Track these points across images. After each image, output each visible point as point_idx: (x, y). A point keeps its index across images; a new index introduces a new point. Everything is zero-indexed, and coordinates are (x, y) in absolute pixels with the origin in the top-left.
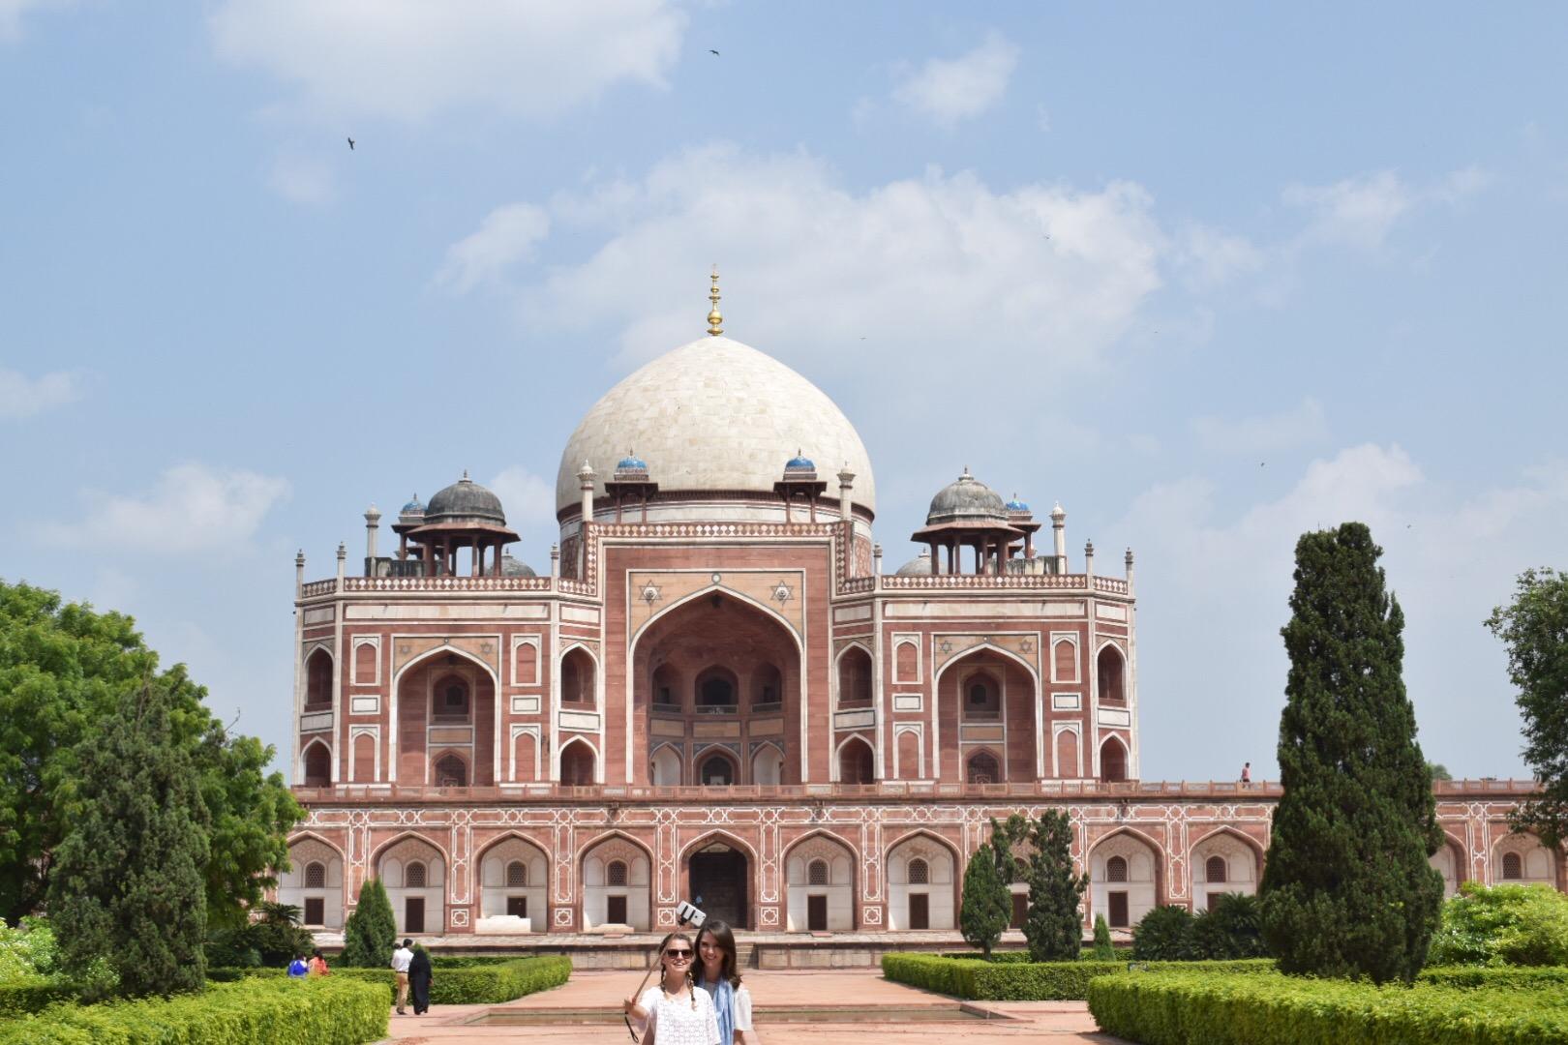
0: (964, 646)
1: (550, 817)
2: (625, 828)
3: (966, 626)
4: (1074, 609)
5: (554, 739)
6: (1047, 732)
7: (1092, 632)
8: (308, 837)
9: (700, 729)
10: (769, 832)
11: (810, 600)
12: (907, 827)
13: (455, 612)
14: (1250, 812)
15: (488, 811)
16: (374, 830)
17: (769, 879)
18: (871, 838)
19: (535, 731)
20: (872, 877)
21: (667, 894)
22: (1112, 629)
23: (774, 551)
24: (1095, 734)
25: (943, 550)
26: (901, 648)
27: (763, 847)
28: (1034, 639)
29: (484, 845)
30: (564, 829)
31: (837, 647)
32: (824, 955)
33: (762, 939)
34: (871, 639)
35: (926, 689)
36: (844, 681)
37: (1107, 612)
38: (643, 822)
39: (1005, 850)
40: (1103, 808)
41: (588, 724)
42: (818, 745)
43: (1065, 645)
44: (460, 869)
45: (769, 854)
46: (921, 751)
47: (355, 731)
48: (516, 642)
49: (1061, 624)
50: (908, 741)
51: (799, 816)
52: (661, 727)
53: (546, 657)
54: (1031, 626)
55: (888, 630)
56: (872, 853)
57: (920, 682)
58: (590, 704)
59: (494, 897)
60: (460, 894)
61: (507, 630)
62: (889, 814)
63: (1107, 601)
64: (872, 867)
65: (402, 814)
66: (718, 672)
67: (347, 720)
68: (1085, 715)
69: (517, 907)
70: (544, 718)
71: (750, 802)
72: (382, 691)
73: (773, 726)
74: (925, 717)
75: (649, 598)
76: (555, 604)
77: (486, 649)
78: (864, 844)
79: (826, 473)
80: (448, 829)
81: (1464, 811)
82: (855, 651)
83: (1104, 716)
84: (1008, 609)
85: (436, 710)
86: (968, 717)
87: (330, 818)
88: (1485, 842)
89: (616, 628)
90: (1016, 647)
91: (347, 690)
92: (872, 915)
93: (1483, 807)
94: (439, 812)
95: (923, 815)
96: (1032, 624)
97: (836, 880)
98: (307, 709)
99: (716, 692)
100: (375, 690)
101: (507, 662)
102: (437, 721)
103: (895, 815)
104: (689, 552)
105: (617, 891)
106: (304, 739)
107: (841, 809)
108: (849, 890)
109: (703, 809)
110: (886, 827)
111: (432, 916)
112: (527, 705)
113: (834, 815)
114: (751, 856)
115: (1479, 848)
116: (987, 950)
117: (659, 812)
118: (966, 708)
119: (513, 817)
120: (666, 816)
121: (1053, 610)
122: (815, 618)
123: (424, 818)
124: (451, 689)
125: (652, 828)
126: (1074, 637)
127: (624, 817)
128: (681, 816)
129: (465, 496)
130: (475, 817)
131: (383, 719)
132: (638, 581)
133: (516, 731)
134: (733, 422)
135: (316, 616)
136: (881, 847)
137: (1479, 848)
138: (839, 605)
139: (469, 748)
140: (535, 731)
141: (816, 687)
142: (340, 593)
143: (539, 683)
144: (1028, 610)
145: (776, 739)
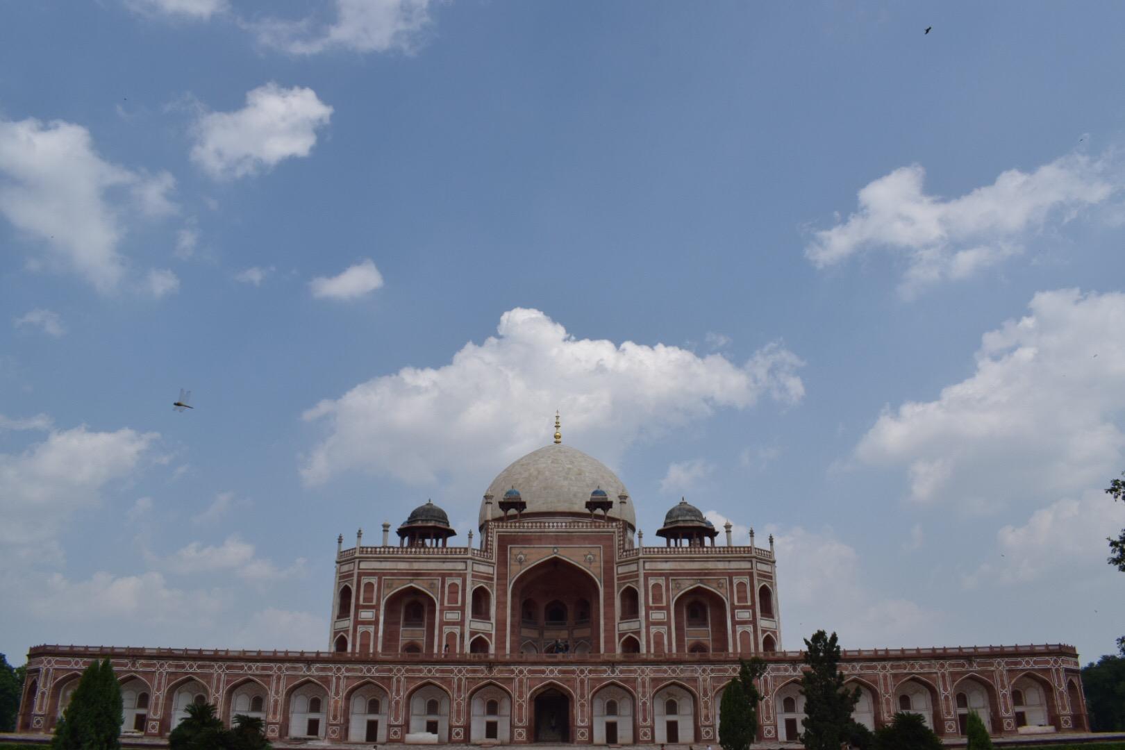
0: (688, 585)
1: (452, 672)
2: (496, 679)
4: (746, 565)
5: (467, 635)
6: (734, 632)
7: (756, 577)
8: (308, 682)
9: (547, 634)
10: (582, 682)
11: (605, 562)
12: (665, 679)
13: (416, 566)
14: (869, 668)
15: (415, 667)
16: (348, 678)
17: (582, 711)
18: (644, 686)
19: (457, 630)
20: (644, 710)
21: (520, 720)
22: (765, 576)
23: (585, 538)
24: (759, 633)
25: (672, 541)
27: (579, 691)
28: (725, 581)
29: (412, 688)
30: (460, 680)
31: (619, 587)
34: (637, 582)
35: (667, 608)
36: (623, 606)
38: (507, 675)
39: (750, 682)
40: (782, 666)
41: (486, 627)
42: (610, 641)
43: (741, 584)
44: (397, 703)
45: (582, 696)
46: (666, 642)
47: (360, 629)
48: (449, 581)
49: (740, 573)
50: (659, 637)
51: (601, 672)
52: (526, 632)
54: (723, 574)
55: (646, 576)
56: (644, 695)
58: (486, 617)
59: (418, 722)
60: (396, 719)
61: (444, 576)
62: (655, 671)
63: (762, 561)
64: (644, 704)
65: (364, 668)
66: (557, 599)
67: (357, 623)
68: (754, 622)
69: (432, 727)
70: (461, 623)
71: (571, 663)
72: (376, 607)
73: (586, 632)
74: (668, 624)
75: (520, 562)
76: (470, 562)
77: (432, 586)
78: (640, 689)
79: (612, 497)
81: (992, 665)
83: (763, 623)
84: (710, 565)
85: (406, 619)
86: (690, 625)
87: (323, 670)
89: (502, 577)
90: (715, 585)
91: (358, 607)
92: (645, 734)
93: (1003, 661)
94: (386, 667)
95: (674, 671)
98: (338, 617)
99: (556, 615)
101: (443, 593)
102: (406, 625)
103: (658, 671)
104: (541, 538)
105: (492, 718)
106: (336, 633)
107: (625, 668)
108: (630, 719)
109: (543, 668)
110: (653, 680)
112: (453, 616)
113: (621, 672)
114: (571, 696)
115: (1003, 687)
117: (516, 668)
118: (688, 620)
119: (430, 671)
120: (521, 672)
121: (734, 565)
122: (608, 572)
123: (377, 671)
124: (412, 606)
125: (512, 679)
126: (746, 580)
127: (496, 673)
129: (428, 510)
131: (376, 623)
132: (515, 551)
133: (447, 630)
134: (565, 479)
135: (345, 568)
136: (650, 691)
137: (1003, 687)
138: (620, 564)
139: (422, 640)
140: (457, 630)
141: (608, 608)
142: (357, 555)
143: (460, 604)
144: (721, 565)
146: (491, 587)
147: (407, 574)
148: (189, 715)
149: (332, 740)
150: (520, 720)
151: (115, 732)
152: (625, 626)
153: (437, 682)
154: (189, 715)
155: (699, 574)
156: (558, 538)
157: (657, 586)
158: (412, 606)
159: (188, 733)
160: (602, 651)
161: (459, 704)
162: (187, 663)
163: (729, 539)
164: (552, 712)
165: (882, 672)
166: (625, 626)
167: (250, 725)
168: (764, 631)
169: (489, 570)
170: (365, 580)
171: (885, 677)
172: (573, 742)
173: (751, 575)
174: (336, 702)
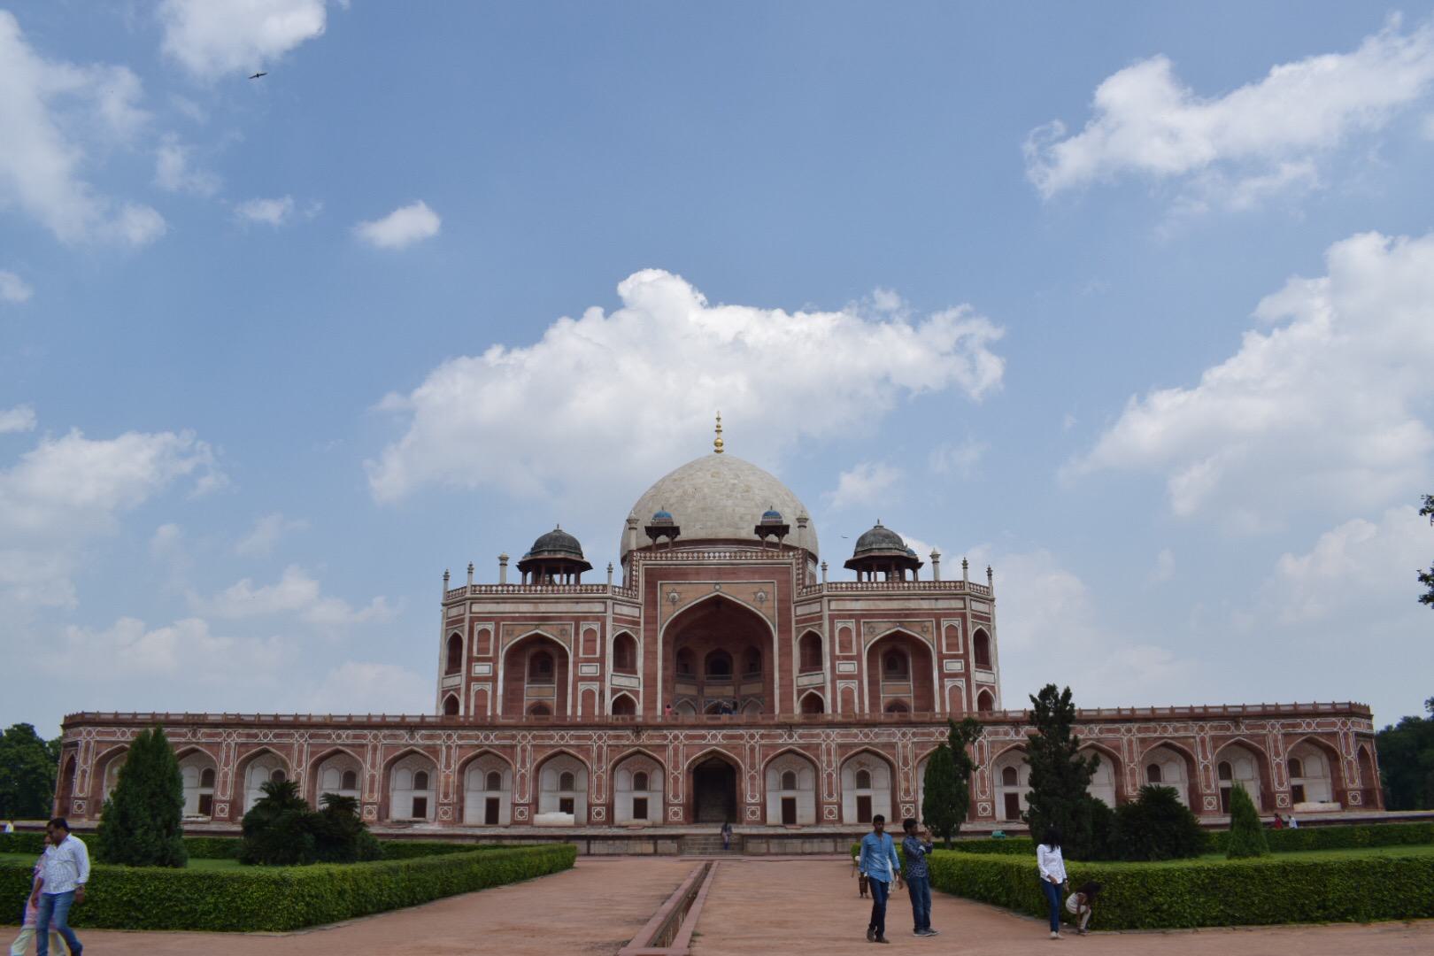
0: (884, 629)
1: (590, 738)
3: (885, 615)
4: (958, 604)
5: (608, 694)
6: (942, 687)
7: (970, 620)
8: (412, 752)
9: (708, 691)
10: (752, 749)
11: (780, 601)
12: (855, 745)
13: (543, 608)
14: (1109, 731)
15: (544, 733)
16: (460, 747)
18: (829, 754)
19: (595, 687)
20: (830, 784)
22: (981, 618)
23: (755, 571)
25: (865, 574)
26: (842, 630)
27: (748, 760)
30: (600, 748)
31: (798, 631)
32: (796, 845)
33: (747, 831)
34: (821, 625)
35: (858, 658)
36: (803, 655)
37: (980, 607)
38: (658, 742)
39: (961, 748)
40: (1001, 729)
41: (632, 683)
43: (951, 628)
44: (523, 777)
45: (753, 766)
47: (475, 687)
48: (584, 627)
49: (949, 614)
50: (847, 693)
51: (775, 737)
52: (681, 689)
53: (603, 637)
54: (929, 615)
55: (832, 618)
56: (830, 763)
57: (854, 653)
59: (549, 799)
60: (522, 796)
61: (577, 620)
62: (842, 736)
64: (830, 775)
65: (481, 735)
66: (720, 647)
68: (967, 675)
69: (567, 806)
70: (601, 678)
71: (739, 726)
72: (494, 660)
74: (859, 677)
75: (674, 601)
76: (610, 603)
77: (563, 633)
78: (824, 758)
79: (788, 519)
80: (513, 747)
81: (1264, 727)
82: (810, 634)
83: (979, 676)
84: (912, 604)
85: (532, 674)
86: (887, 678)
87: (430, 737)
88: (1281, 749)
89: (651, 620)
91: (470, 660)
92: (831, 812)
93: (1278, 723)
94: (508, 733)
95: (866, 736)
96: (931, 614)
97: (803, 786)
99: (719, 667)
100: (489, 660)
101: (577, 640)
102: (532, 681)
103: (847, 736)
105: (640, 795)
106: (444, 693)
107: (806, 731)
108: (812, 794)
110: (840, 746)
111: (504, 815)
112: (589, 670)
113: (801, 737)
115: (1277, 754)
116: (947, 837)
117: (671, 734)
118: (885, 672)
120: (676, 737)
121: (942, 604)
122: (784, 613)
123: (497, 738)
124: (539, 657)
125: (664, 747)
126: (957, 622)
127: (645, 738)
128: (687, 737)
129: (556, 539)
130: (534, 738)
131: (494, 679)
132: (666, 589)
133: (582, 687)
134: (729, 497)
135: (454, 612)
136: (836, 761)
137: (1277, 754)
139: (552, 700)
140: (595, 687)
141: (785, 660)
144: (925, 605)
145: (757, 696)
146: (637, 633)
147: (533, 619)
148: (265, 795)
149: (444, 823)
150: (676, 796)
151: (176, 816)
152: (805, 681)
153: (571, 751)
154: (265, 795)
155: (899, 616)
156: (720, 572)
157: (845, 631)
158: (539, 657)
159: (265, 818)
160: (777, 711)
161: (599, 778)
162: (261, 732)
163: (936, 572)
164: (715, 785)
165: (1126, 737)
166: (805, 681)
167: (342, 806)
168: (979, 686)
169: (635, 612)
170: (479, 627)
171: (1130, 743)
172: (741, 822)
173: (964, 616)
174: (447, 777)
